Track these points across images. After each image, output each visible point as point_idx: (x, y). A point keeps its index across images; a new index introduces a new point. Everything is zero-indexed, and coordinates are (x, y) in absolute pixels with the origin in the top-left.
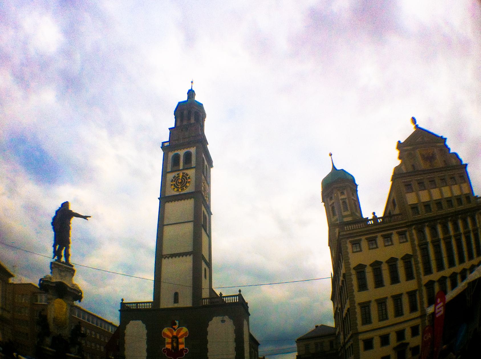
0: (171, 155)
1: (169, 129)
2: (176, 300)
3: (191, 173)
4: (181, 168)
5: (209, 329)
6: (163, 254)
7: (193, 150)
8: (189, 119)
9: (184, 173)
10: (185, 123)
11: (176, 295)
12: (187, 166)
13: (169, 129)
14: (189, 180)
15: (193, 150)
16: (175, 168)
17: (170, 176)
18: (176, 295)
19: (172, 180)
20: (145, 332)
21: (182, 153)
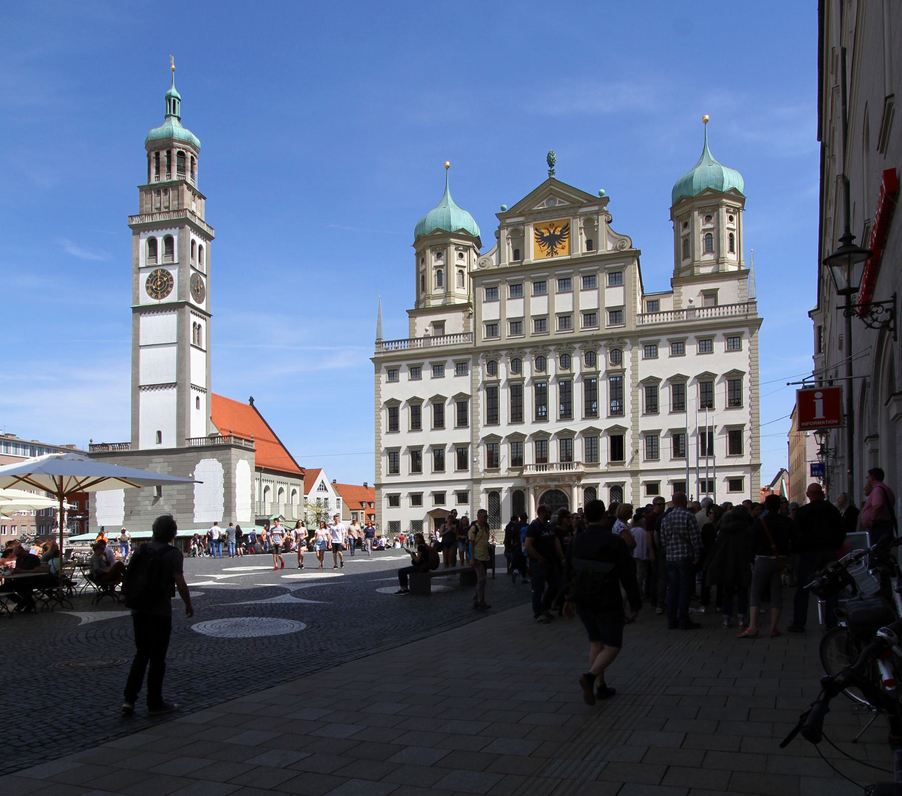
3: (174, 272)
4: (160, 263)
6: (141, 384)
9: (163, 271)
15: (175, 233)
19: (148, 280)
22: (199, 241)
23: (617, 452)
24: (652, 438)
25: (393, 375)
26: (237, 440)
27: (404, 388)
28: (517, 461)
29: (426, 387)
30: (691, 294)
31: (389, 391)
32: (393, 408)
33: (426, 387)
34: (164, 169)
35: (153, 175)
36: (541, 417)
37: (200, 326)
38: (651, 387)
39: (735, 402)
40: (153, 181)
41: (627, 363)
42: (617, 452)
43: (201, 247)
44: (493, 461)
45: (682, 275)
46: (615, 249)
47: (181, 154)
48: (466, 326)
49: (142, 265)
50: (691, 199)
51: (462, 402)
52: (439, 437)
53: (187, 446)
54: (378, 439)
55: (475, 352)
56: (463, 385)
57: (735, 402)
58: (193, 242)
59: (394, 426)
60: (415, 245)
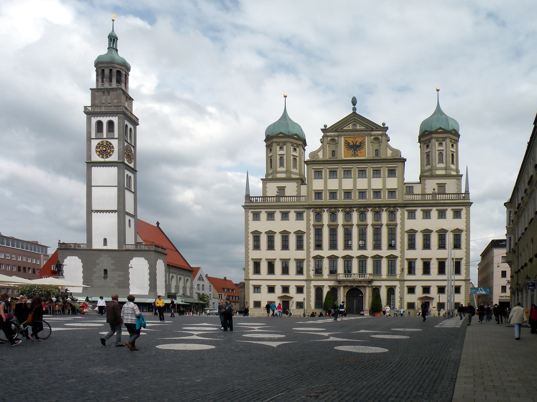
0: (94, 120)
1: (91, 89)
3: (115, 143)
4: (105, 136)
7: (115, 119)
8: (111, 81)
10: (107, 85)
12: (110, 135)
13: (91, 89)
14: (112, 149)
15: (115, 119)
16: (99, 135)
17: (95, 143)
21: (105, 120)
22: (130, 126)
23: (392, 270)
24: (411, 264)
25: (256, 216)
26: (157, 248)
27: (263, 225)
28: (333, 272)
29: (278, 225)
30: (431, 185)
31: (254, 226)
32: (257, 236)
33: (278, 225)
35: (100, 83)
36: (348, 246)
37: (130, 177)
38: (412, 234)
39: (457, 246)
40: (100, 87)
41: (398, 221)
42: (392, 270)
43: (131, 129)
44: (318, 271)
45: (425, 174)
46: (392, 155)
47: (119, 72)
48: (299, 190)
50: (431, 133)
51: (300, 235)
52: (285, 255)
53: (124, 249)
54: (247, 253)
55: (309, 207)
56: (301, 226)
57: (457, 246)
58: (126, 126)
59: (257, 247)
60: (266, 141)
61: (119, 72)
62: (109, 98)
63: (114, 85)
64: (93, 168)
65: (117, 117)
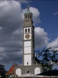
0: (25, 29)
2: (28, 64)
4: (27, 33)
5: (35, 70)
8: (28, 18)
10: (28, 19)
11: (28, 63)
12: (29, 32)
15: (30, 28)
16: (26, 33)
17: (25, 35)
18: (28, 63)
20: (21, 71)
21: (27, 28)
34: (27, 18)
40: (26, 20)
49: (24, 33)
61: (30, 16)
62: (28, 23)
63: (29, 19)
64: (25, 42)
65: (31, 28)
